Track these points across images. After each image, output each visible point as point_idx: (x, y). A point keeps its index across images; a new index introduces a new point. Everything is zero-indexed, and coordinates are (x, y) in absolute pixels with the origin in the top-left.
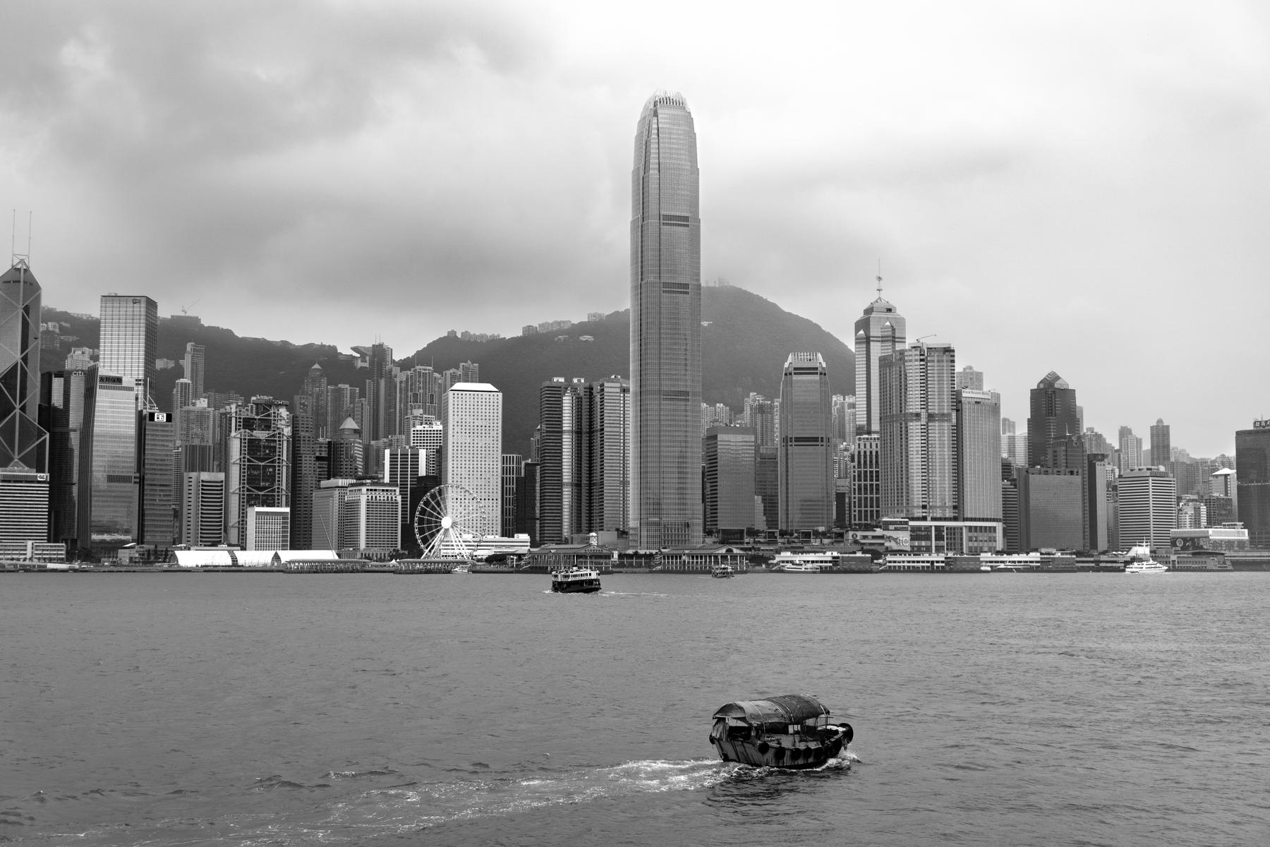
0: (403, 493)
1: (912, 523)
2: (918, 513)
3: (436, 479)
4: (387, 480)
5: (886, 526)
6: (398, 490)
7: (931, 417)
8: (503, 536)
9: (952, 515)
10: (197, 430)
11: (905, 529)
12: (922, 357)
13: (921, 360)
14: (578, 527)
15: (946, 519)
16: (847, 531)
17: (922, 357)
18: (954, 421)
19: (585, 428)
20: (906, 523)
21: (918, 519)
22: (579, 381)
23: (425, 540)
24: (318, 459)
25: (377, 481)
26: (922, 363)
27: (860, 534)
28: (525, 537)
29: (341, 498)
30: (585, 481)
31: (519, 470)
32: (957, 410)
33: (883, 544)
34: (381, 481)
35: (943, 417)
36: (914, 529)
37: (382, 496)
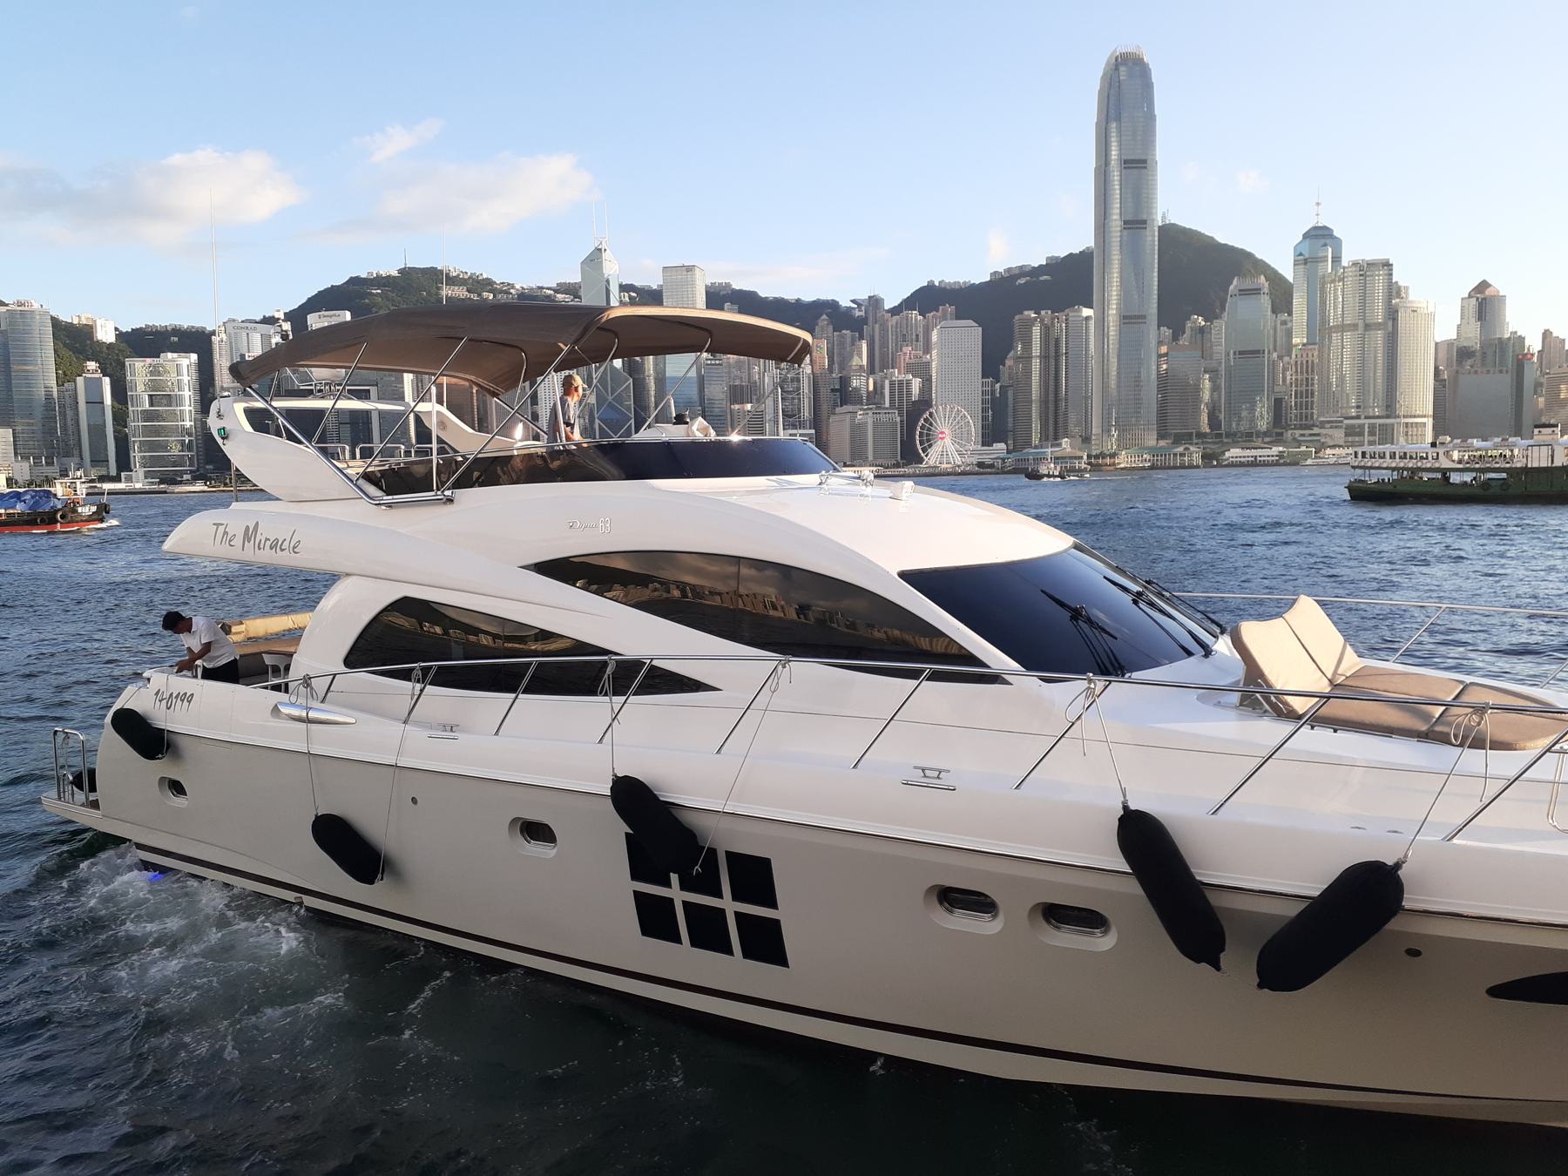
0: (900, 414)
1: (1346, 422)
2: (1353, 412)
3: (925, 403)
4: (887, 405)
5: (1322, 425)
6: (897, 412)
7: (1367, 327)
8: (983, 445)
9: (1384, 413)
10: (735, 372)
11: (1341, 427)
12: (1361, 273)
13: (1361, 275)
14: (1045, 437)
15: (1378, 417)
16: (1287, 431)
17: (1361, 273)
18: (1390, 329)
19: (1052, 353)
20: (1341, 422)
21: (1352, 418)
22: (1046, 313)
23: (924, 450)
24: (832, 390)
25: (879, 405)
26: (1361, 278)
27: (1298, 432)
28: (1002, 446)
29: (853, 420)
30: (1051, 397)
31: (993, 392)
32: (1394, 319)
33: (1319, 441)
34: (883, 406)
35: (1378, 326)
36: (1348, 427)
37: (884, 418)
